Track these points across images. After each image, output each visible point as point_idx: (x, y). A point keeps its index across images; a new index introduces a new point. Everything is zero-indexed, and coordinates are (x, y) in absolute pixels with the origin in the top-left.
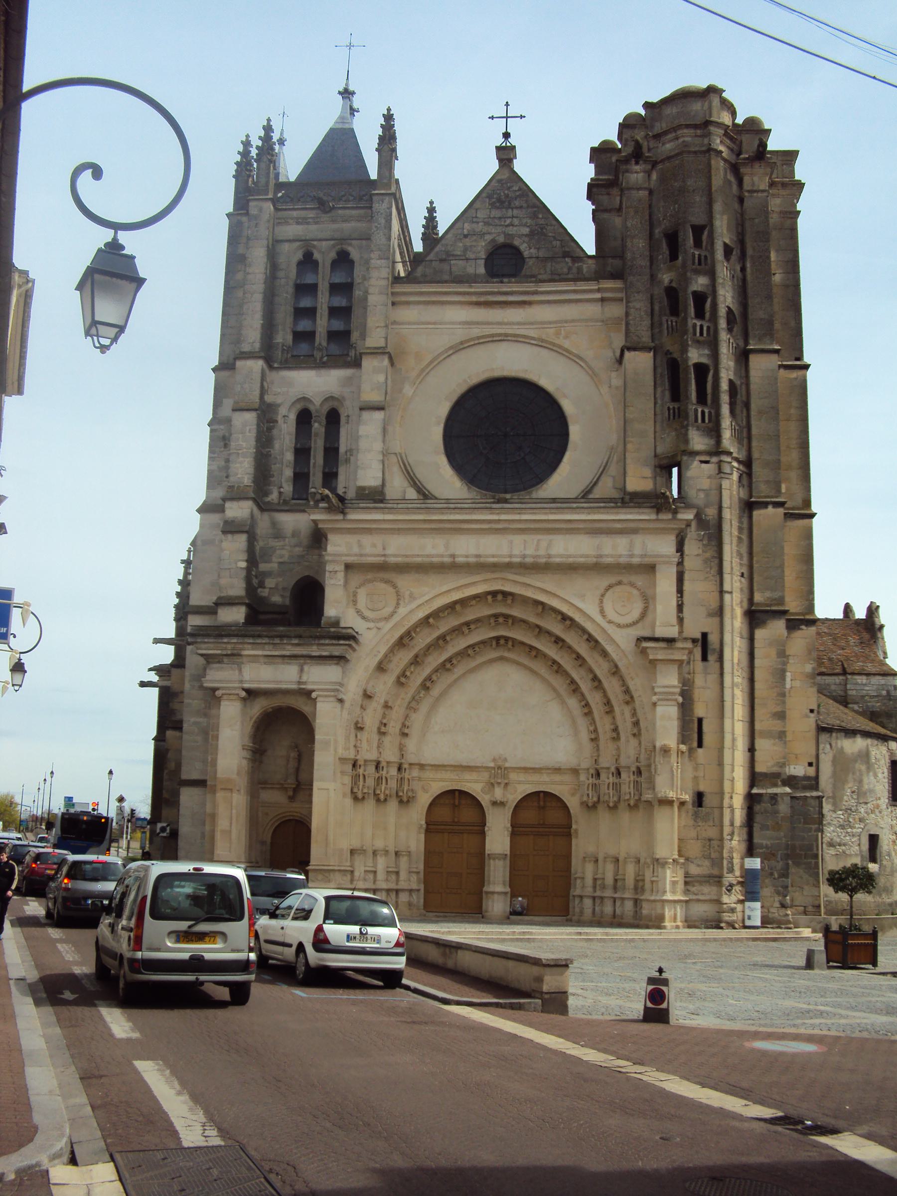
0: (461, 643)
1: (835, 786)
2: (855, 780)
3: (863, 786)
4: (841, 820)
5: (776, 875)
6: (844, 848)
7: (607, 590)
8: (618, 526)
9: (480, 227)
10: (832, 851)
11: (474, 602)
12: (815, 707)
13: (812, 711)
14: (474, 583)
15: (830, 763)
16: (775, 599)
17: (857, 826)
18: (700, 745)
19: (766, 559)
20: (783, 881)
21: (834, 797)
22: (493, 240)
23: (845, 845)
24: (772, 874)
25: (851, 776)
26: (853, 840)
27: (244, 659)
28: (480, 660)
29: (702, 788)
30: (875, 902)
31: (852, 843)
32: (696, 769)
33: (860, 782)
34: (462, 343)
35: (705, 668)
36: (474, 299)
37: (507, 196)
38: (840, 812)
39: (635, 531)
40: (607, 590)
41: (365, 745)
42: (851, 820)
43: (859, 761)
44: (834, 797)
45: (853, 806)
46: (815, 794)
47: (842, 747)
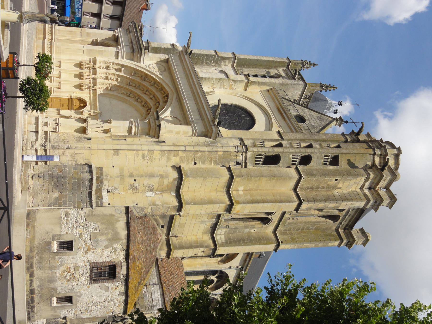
0: (146, 98)
1: (98, 216)
2: (103, 229)
3: (100, 235)
4: (80, 220)
5: (50, 173)
6: (65, 222)
7: (176, 118)
8: (203, 114)
9: (308, 114)
10: (63, 215)
11: (162, 92)
12: (138, 206)
13: (137, 204)
14: (169, 87)
15: (110, 213)
16: (187, 174)
17: (77, 231)
18: (113, 140)
19: (205, 171)
20: (47, 175)
21: (92, 215)
22: (305, 116)
23: (67, 224)
24: (51, 171)
25: (105, 226)
26: (69, 228)
27: (129, 35)
28: (141, 108)
29: (92, 139)
30: (34, 247)
31: (68, 228)
32: (102, 138)
33: (102, 234)
34: (262, 106)
35: (149, 142)
36: (279, 106)
37: (323, 120)
38: (85, 220)
39: (203, 119)
40: (176, 118)
41: (102, 70)
42: (81, 227)
43: (113, 232)
44: (92, 215)
45: (88, 229)
46: (94, 204)
47: (119, 221)
